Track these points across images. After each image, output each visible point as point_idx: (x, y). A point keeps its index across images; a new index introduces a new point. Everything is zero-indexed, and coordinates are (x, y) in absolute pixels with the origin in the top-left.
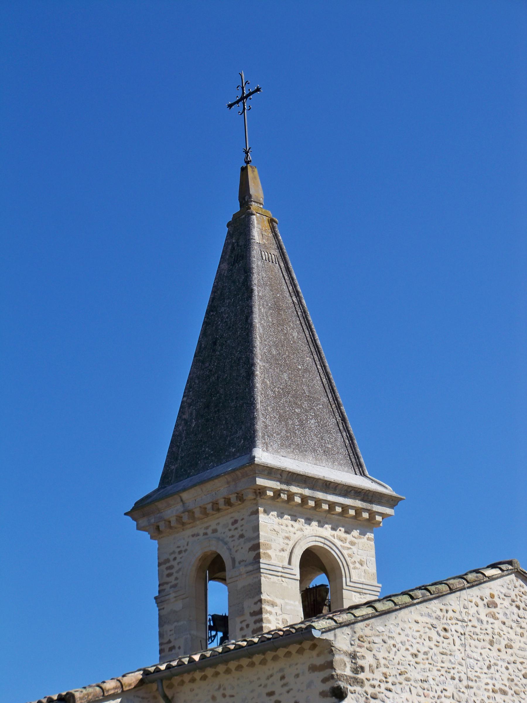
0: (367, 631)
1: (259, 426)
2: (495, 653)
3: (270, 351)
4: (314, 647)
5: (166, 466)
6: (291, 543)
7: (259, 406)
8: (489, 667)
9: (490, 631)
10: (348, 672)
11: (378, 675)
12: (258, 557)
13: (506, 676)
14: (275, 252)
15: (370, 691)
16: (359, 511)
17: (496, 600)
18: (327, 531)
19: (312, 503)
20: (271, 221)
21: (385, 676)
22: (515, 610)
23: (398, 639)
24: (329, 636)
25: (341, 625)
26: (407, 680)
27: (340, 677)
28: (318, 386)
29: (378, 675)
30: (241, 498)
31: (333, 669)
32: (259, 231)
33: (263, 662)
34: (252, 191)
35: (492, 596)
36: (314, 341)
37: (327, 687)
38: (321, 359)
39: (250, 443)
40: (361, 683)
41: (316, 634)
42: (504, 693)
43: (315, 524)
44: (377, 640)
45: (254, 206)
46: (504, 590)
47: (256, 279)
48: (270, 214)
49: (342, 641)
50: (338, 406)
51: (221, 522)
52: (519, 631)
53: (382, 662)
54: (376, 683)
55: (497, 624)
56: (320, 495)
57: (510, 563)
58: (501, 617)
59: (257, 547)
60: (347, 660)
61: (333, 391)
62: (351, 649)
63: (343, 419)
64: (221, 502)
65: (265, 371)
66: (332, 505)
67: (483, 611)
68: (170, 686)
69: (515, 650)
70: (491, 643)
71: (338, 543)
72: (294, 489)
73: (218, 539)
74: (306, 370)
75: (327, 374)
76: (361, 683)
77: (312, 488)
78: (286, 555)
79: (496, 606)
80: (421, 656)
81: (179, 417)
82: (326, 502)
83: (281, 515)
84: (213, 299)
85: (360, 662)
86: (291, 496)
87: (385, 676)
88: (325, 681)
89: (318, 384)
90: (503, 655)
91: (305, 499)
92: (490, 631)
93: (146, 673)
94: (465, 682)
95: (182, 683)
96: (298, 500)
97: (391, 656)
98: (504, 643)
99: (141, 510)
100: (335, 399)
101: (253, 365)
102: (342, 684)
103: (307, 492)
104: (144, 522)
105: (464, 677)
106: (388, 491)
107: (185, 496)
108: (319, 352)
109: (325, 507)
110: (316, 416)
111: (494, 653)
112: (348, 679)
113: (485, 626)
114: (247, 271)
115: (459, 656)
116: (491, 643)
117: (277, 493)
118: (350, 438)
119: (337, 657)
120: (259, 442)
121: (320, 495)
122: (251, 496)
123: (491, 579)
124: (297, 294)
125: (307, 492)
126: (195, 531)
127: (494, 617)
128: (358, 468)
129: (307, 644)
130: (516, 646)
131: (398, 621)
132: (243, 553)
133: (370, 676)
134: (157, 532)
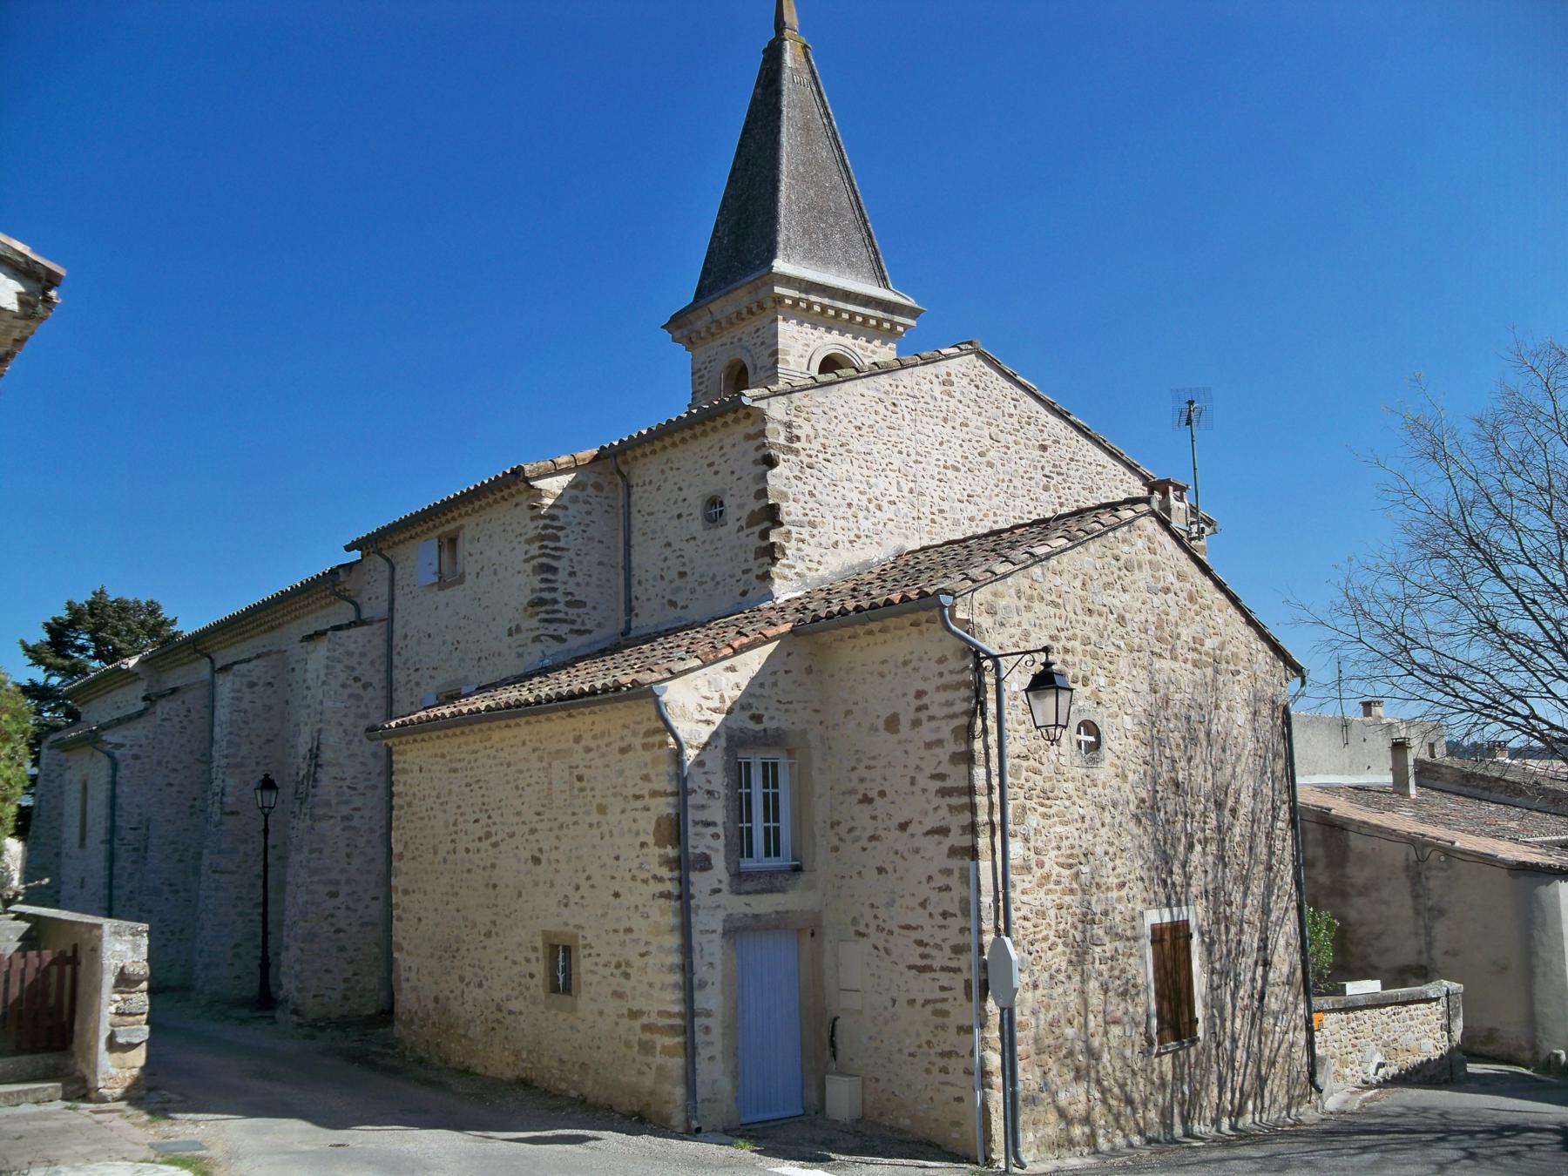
0: (806, 401)
1: (781, 238)
2: (948, 430)
3: (796, 169)
4: (748, 416)
5: (701, 281)
6: (811, 350)
7: (781, 220)
8: (941, 444)
9: (944, 408)
10: (782, 440)
11: (816, 445)
12: (777, 362)
13: (960, 452)
14: (807, 76)
15: (806, 460)
16: (880, 321)
17: (953, 378)
18: (848, 340)
19: (831, 312)
20: (805, 47)
21: (824, 446)
22: (974, 390)
23: (840, 411)
24: (762, 404)
25: (776, 394)
26: (849, 451)
27: (772, 445)
28: (846, 204)
29: (816, 445)
30: (761, 307)
31: (765, 436)
32: (791, 56)
33: (705, 434)
34: (786, 18)
35: (949, 374)
36: (843, 161)
37: (759, 455)
38: (849, 178)
39: (772, 254)
40: (796, 452)
41: (746, 401)
42: (957, 470)
43: (835, 333)
44: (818, 411)
45: (787, 33)
46: (963, 370)
47: (785, 100)
48: (804, 40)
49: (776, 410)
50: (865, 223)
51: (745, 330)
52: (977, 410)
53: (822, 432)
54: (813, 453)
55: (953, 402)
56: (840, 305)
57: (970, 343)
58: (958, 395)
59: (776, 352)
60: (781, 428)
61: (860, 208)
62: (787, 419)
63: (870, 235)
64: (744, 311)
65: (791, 187)
66: (852, 315)
67: (938, 389)
68: (626, 462)
69: (971, 428)
70: (945, 420)
71: (859, 352)
72: (813, 298)
73: (742, 347)
74: (833, 188)
75: (855, 192)
76: (796, 452)
77: (832, 297)
78: (805, 361)
79: (952, 384)
80: (865, 429)
81: (714, 235)
82: (846, 311)
83: (800, 323)
84: (747, 123)
85: (796, 432)
86: (810, 305)
87: (824, 446)
88: (758, 449)
89: (845, 200)
90: (957, 433)
91: (824, 308)
92: (944, 408)
93: (603, 448)
94: (914, 457)
95: (635, 458)
96: (817, 308)
97: (832, 427)
98: (959, 421)
99: (677, 322)
100: (862, 215)
101: (778, 181)
102: (773, 452)
103: (826, 301)
104: (678, 334)
105: (912, 452)
106: (911, 302)
107: (713, 307)
108: (847, 171)
109: (846, 316)
110: (841, 231)
111: (948, 430)
112: (781, 448)
113: (939, 403)
114: (778, 93)
115: (908, 431)
116: (945, 420)
117: (796, 302)
118: (876, 253)
119: (769, 425)
120: (780, 253)
121: (840, 305)
122: (769, 304)
123: (948, 357)
124: (828, 116)
125: (826, 301)
126: (724, 340)
127: (949, 394)
128: (882, 281)
129: (741, 413)
130: (972, 424)
131: (842, 393)
132: (764, 361)
133: (807, 446)
134: (690, 344)
